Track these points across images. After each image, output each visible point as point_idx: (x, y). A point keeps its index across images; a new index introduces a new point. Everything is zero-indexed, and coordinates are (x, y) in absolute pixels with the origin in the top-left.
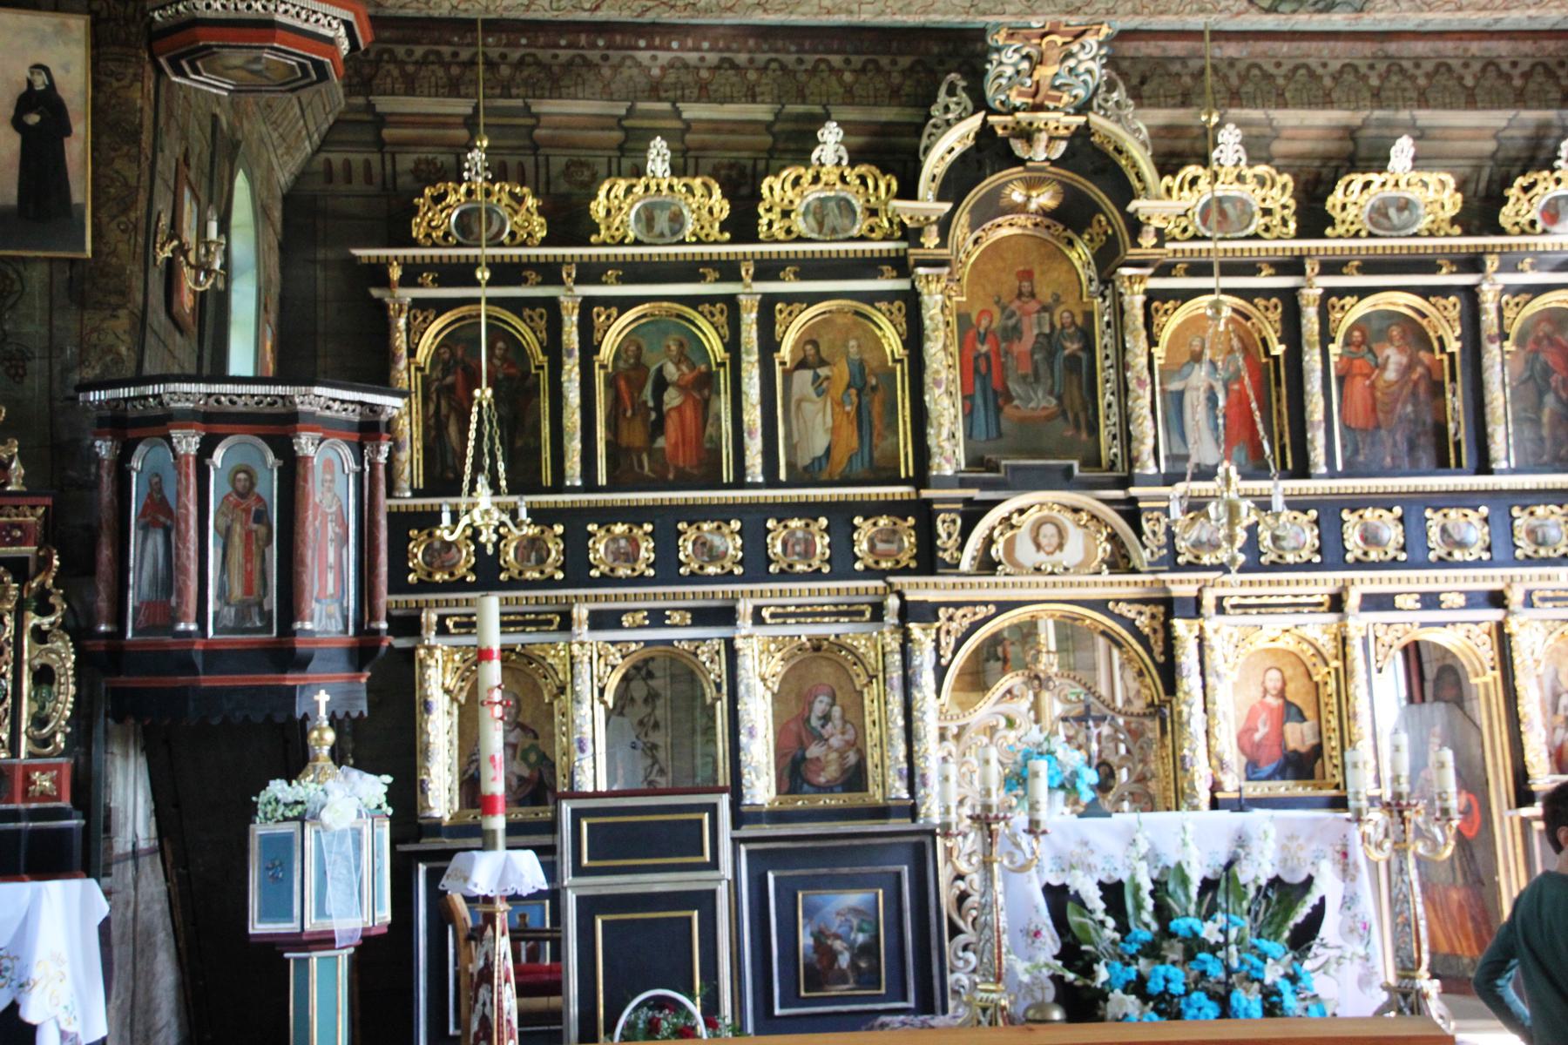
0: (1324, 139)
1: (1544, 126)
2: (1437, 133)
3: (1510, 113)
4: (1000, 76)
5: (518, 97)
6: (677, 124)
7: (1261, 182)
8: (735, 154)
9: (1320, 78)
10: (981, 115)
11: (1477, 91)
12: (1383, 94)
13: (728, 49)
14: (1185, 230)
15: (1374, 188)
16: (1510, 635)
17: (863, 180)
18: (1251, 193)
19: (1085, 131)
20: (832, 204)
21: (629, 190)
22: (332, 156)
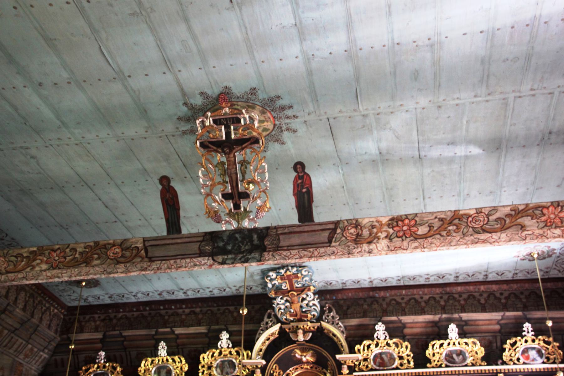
0: (425, 327)
1: (516, 318)
2: (471, 323)
3: (502, 314)
4: (280, 309)
5: (117, 330)
6: (173, 336)
7: (397, 345)
8: (195, 346)
9: (420, 303)
10: (279, 325)
11: (486, 305)
12: (446, 308)
13: (192, 307)
14: (367, 367)
15: (445, 345)
17: (238, 353)
18: (394, 351)
19: (321, 330)
20: (226, 363)
21: (152, 362)
22: (57, 357)
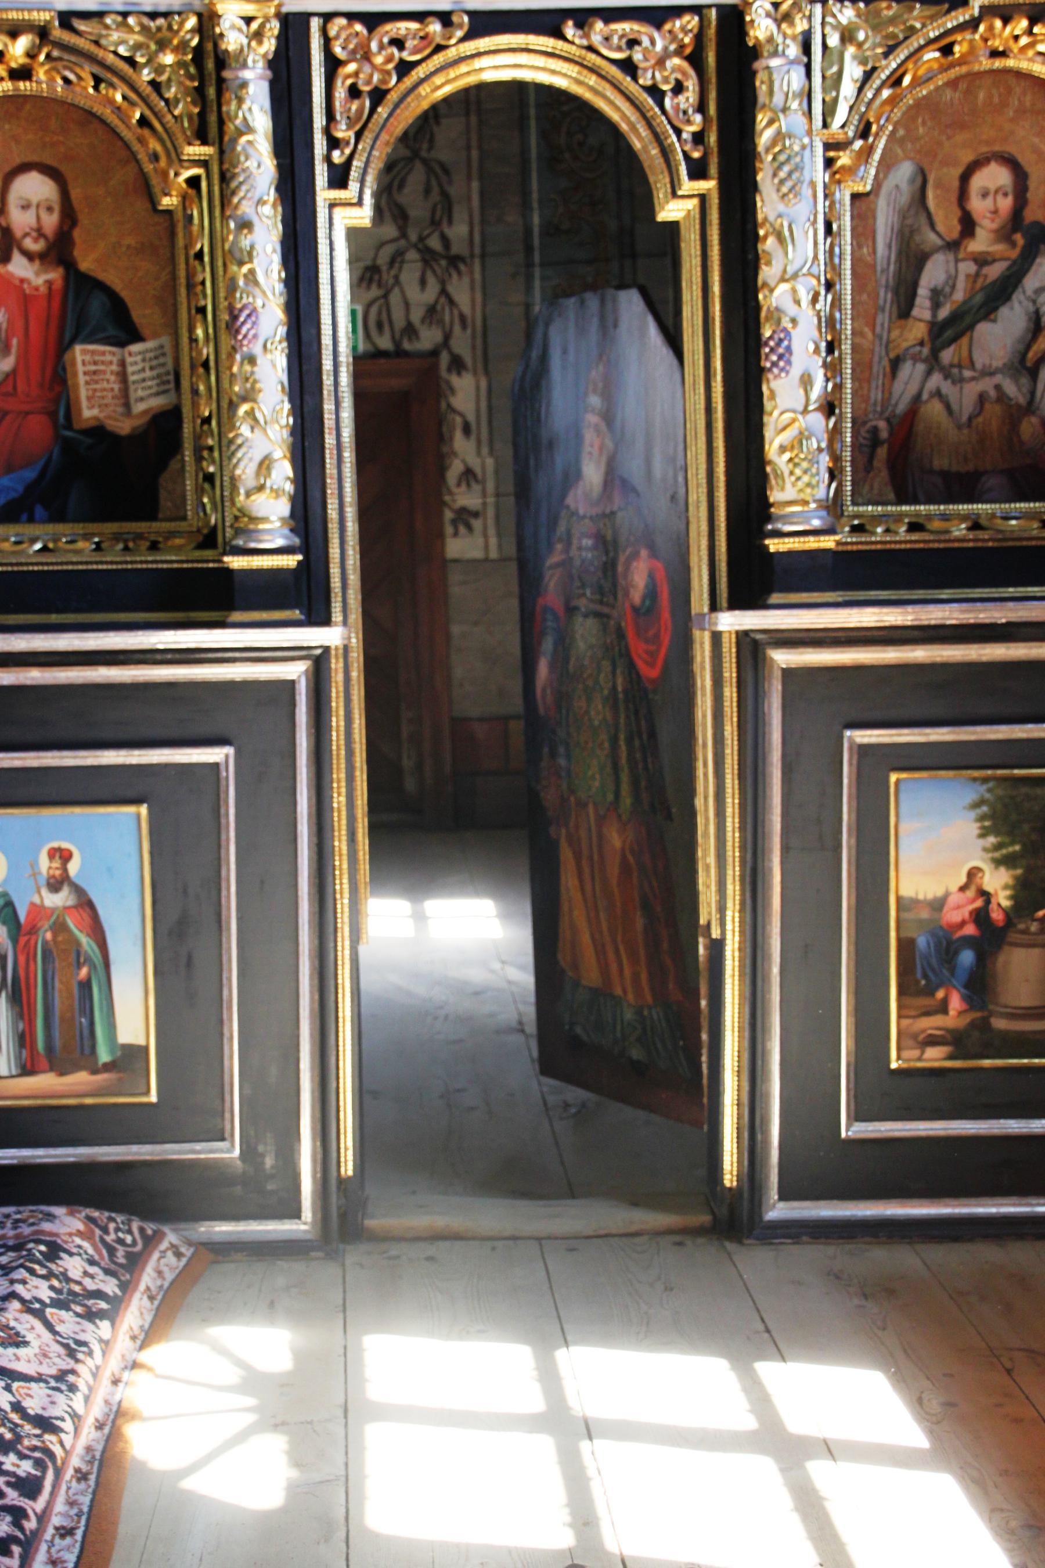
16: (755, 53)
